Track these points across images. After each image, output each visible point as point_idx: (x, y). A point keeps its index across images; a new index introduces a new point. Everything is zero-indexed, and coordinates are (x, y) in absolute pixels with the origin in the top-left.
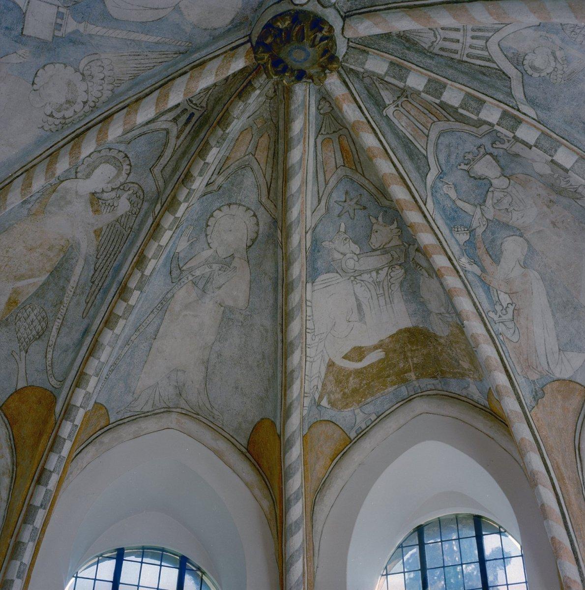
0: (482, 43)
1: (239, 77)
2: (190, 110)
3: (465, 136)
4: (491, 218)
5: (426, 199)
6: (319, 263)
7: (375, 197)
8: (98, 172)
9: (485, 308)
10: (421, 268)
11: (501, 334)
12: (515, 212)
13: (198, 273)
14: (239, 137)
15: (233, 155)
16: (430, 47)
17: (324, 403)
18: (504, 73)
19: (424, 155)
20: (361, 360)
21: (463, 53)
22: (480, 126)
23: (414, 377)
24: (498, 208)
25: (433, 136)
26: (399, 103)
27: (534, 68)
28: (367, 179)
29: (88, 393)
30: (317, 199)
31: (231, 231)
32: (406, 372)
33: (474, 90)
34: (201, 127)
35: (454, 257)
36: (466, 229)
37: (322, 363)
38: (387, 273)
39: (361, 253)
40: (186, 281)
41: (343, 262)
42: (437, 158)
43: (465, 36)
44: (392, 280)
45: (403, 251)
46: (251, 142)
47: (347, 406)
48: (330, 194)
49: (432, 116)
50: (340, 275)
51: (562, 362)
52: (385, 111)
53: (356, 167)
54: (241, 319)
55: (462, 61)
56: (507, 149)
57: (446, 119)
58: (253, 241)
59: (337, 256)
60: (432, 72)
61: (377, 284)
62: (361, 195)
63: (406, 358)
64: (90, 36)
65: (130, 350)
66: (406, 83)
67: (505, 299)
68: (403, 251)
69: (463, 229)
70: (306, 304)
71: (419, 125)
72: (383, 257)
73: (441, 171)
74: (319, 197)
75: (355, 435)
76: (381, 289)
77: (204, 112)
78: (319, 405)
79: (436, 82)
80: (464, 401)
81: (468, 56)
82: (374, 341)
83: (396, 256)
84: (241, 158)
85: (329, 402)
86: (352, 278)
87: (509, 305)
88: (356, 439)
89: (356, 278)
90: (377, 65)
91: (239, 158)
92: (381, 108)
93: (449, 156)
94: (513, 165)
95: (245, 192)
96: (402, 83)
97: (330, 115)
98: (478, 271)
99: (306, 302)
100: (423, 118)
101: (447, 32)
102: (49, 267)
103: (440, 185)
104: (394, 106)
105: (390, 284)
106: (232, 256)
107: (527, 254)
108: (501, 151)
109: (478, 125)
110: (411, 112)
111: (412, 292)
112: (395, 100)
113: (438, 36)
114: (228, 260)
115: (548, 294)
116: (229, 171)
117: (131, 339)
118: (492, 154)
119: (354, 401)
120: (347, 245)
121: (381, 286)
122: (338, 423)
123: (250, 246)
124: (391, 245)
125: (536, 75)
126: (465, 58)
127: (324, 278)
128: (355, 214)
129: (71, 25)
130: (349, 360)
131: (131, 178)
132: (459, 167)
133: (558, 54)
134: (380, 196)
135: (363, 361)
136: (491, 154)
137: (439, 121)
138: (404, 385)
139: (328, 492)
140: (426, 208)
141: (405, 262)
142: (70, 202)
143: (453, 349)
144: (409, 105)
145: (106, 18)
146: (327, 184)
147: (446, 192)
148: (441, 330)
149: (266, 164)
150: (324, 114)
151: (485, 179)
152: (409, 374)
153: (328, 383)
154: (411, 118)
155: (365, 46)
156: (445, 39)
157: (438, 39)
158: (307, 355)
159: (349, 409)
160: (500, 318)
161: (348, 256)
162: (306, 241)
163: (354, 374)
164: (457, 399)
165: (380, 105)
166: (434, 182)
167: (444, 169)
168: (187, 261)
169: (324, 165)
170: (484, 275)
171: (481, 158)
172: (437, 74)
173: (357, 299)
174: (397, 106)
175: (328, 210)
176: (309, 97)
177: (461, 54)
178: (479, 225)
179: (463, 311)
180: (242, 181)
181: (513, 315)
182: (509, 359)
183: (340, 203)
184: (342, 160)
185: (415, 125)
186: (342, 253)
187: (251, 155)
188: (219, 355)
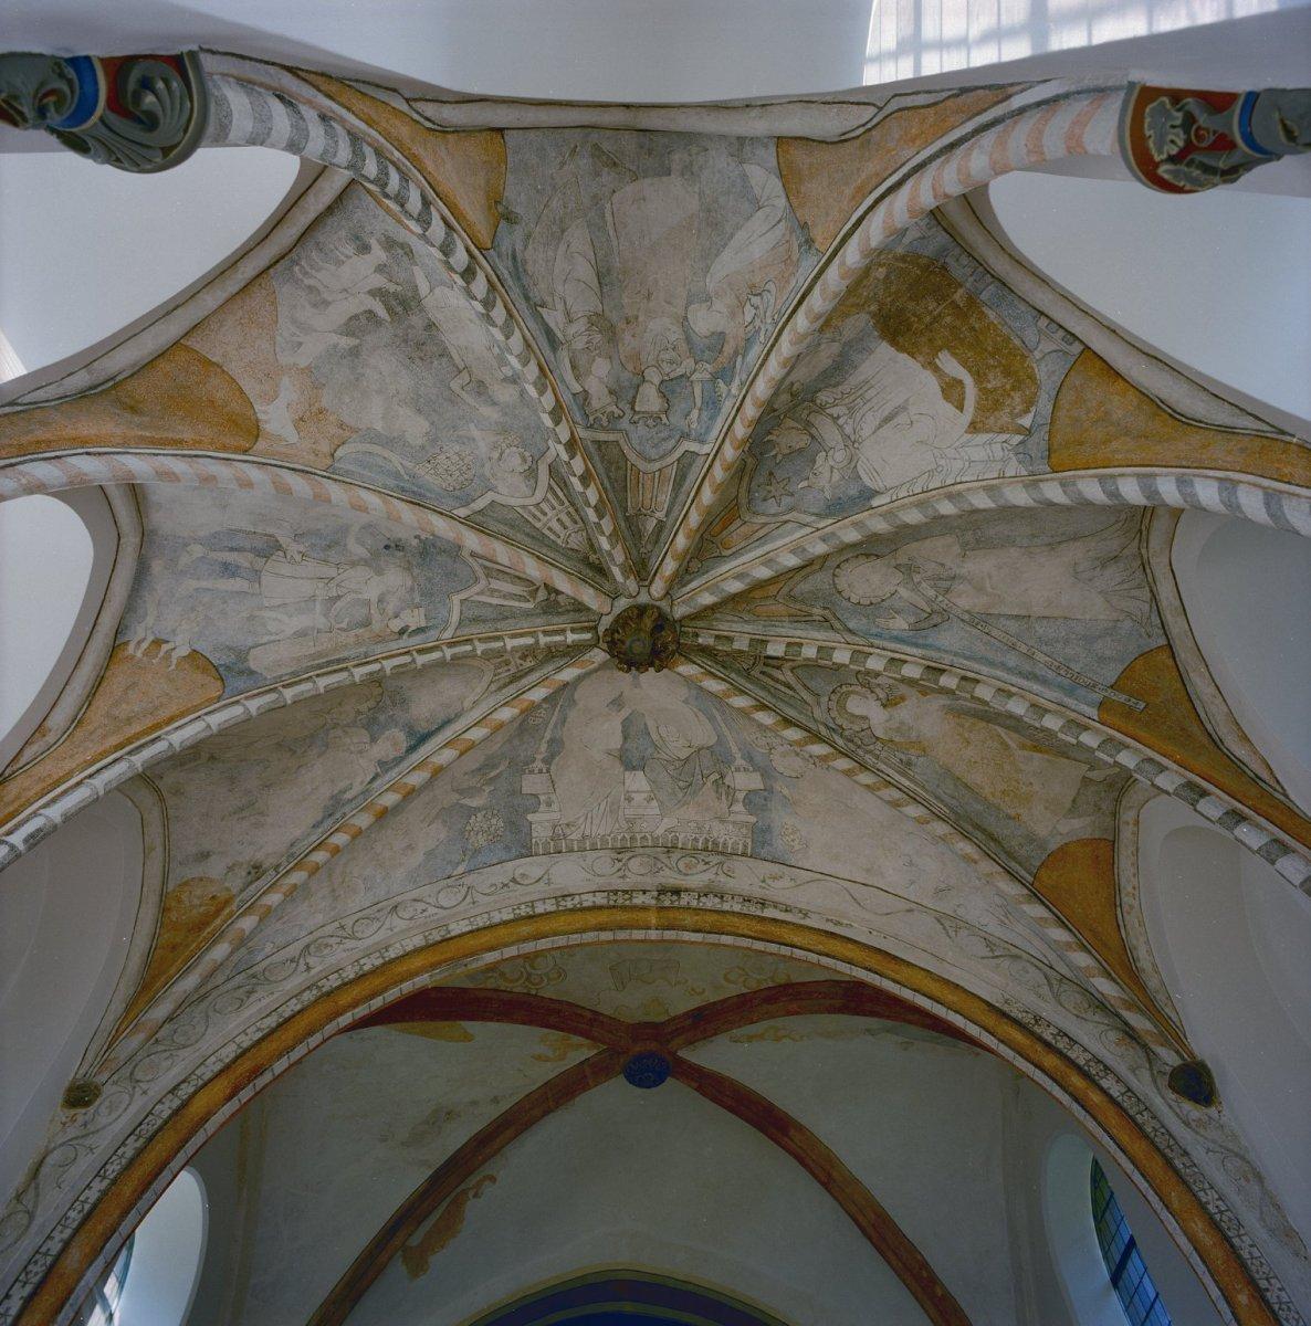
0: (544, 506)
8: (857, 712)
13: (931, 593)
15: (784, 613)
17: (1026, 421)
18: (550, 472)
20: (960, 382)
23: (960, 291)
25: (657, 465)
27: (525, 461)
29: (1061, 730)
32: (958, 306)
37: (973, 443)
40: (946, 602)
41: (841, 465)
43: (549, 520)
47: (1032, 377)
48: (774, 515)
58: (868, 556)
59: (836, 476)
61: (851, 410)
63: (936, 319)
64: (740, 750)
65: (1044, 648)
67: (749, 313)
71: (656, 484)
72: (816, 423)
81: (563, 504)
83: (806, 412)
85: (1027, 411)
93: (663, 439)
94: (626, 383)
100: (649, 484)
102: (984, 724)
111: (839, 368)
116: (804, 607)
117: (1025, 651)
125: (527, 454)
126: (567, 503)
129: (740, 762)
130: (964, 399)
131: (854, 681)
133: (496, 455)
134: (748, 470)
136: (633, 409)
142: (902, 723)
143: (872, 294)
145: (721, 741)
146: (765, 524)
148: (860, 321)
153: (999, 423)
159: (1036, 370)
161: (832, 463)
163: (982, 383)
165: (661, 525)
168: (919, 611)
171: (643, 413)
173: (880, 426)
175: (792, 509)
188: (1034, 536)
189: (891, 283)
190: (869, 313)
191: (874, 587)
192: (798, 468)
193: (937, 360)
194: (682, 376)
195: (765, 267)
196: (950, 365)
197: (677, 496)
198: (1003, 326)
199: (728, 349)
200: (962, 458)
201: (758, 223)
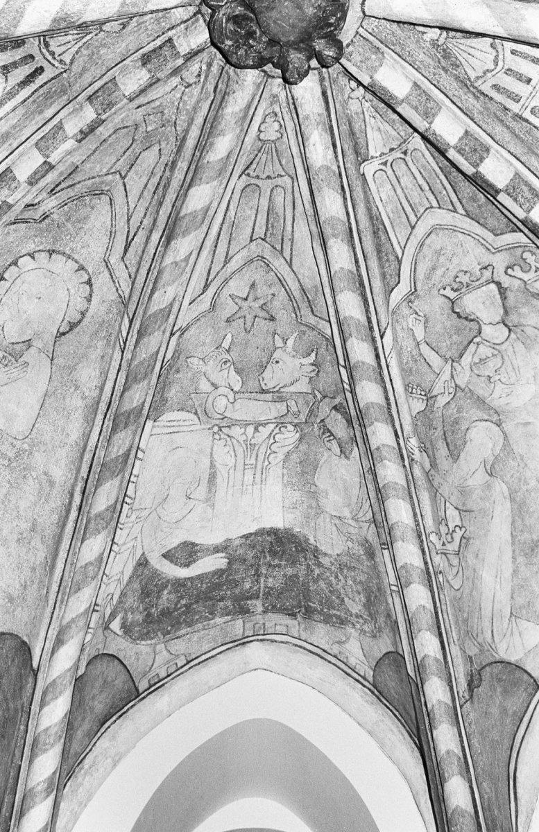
1: (150, 27)
2: (39, 61)
3: (469, 243)
4: (463, 387)
5: (386, 329)
6: (173, 391)
7: (295, 305)
9: (427, 526)
10: (332, 438)
11: (441, 572)
12: (501, 385)
14: (110, 136)
15: (88, 165)
16: (478, 78)
17: (116, 625)
19: (397, 257)
20: (187, 565)
21: (526, 105)
22: (501, 234)
23: (260, 609)
24: (477, 372)
25: (421, 230)
26: (390, 159)
28: (293, 271)
30: (203, 284)
31: (40, 298)
32: (250, 598)
33: (529, 169)
34: (49, 98)
35: (403, 433)
36: (423, 393)
37: (130, 560)
38: (271, 434)
39: (242, 390)
42: (415, 268)
44: (274, 447)
45: (308, 404)
46: (127, 153)
47: (145, 636)
48: (226, 281)
49: (432, 198)
50: (199, 419)
51: (512, 634)
52: (363, 165)
53: (282, 247)
54: (11, 454)
55: (521, 117)
56: (528, 283)
57: (452, 209)
58: (73, 326)
59: (205, 386)
60: (472, 120)
61: (251, 447)
62: (274, 295)
63: (258, 574)
66: (432, 125)
67: (453, 517)
68: (308, 404)
69: (419, 392)
70: (136, 454)
73: (413, 290)
74: (207, 280)
75: (147, 686)
76: (254, 456)
77: (62, 73)
78: (107, 628)
79: (476, 139)
80: (330, 662)
82: (217, 539)
84: (99, 176)
85: (123, 626)
86: (216, 429)
87: (457, 529)
88: (146, 693)
89: (221, 430)
90: (395, 78)
91: (96, 174)
92: (359, 159)
93: (434, 269)
95: (85, 238)
96: (425, 123)
97: (273, 145)
98: (427, 466)
99: (137, 451)
101: (518, 59)
103: (406, 311)
104: (380, 162)
105: (269, 452)
106: (28, 343)
107: (499, 455)
108: (519, 282)
109: (499, 232)
110: (402, 181)
112: (385, 152)
113: (500, 63)
114: (18, 348)
115: (513, 522)
118: (500, 284)
119: (159, 630)
120: (226, 371)
121: (255, 452)
122: (125, 662)
123: (64, 334)
124: (292, 389)
127: (172, 419)
128: (253, 325)
130: (171, 561)
132: (442, 292)
135: (193, 566)
136: (498, 284)
137: (440, 208)
138: (242, 618)
139: (87, 779)
140: (382, 342)
141: (306, 422)
143: (341, 577)
144: (403, 165)
147: (410, 326)
148: (330, 542)
149: (140, 198)
150: (264, 142)
151: (472, 320)
152: (254, 602)
153: (130, 593)
154: (399, 191)
155: (382, 43)
156: (509, 72)
157: (499, 68)
158: (115, 540)
159: (149, 642)
160: (444, 547)
161: (221, 390)
162: (167, 348)
163: (172, 586)
164: (319, 656)
165: (361, 157)
166: (398, 306)
167: (419, 288)
169: (234, 229)
170: (432, 472)
172: (478, 125)
173: (212, 465)
174: (385, 164)
176: (259, 101)
177: (523, 105)
178: (443, 391)
179: (400, 524)
180: (86, 218)
181: (460, 546)
182: (445, 616)
183: (237, 300)
184: (264, 228)
185: (401, 204)
186: (212, 384)
187: (118, 176)
189: (330, 591)
190: (326, 554)
191: (24, 298)
192: (249, 351)
193: (223, 555)
194: (461, 356)
195: (473, 582)
196: (209, 564)
197: (369, 209)
198: (204, 626)
199: (442, 451)
200: (124, 544)
201: (503, 597)
